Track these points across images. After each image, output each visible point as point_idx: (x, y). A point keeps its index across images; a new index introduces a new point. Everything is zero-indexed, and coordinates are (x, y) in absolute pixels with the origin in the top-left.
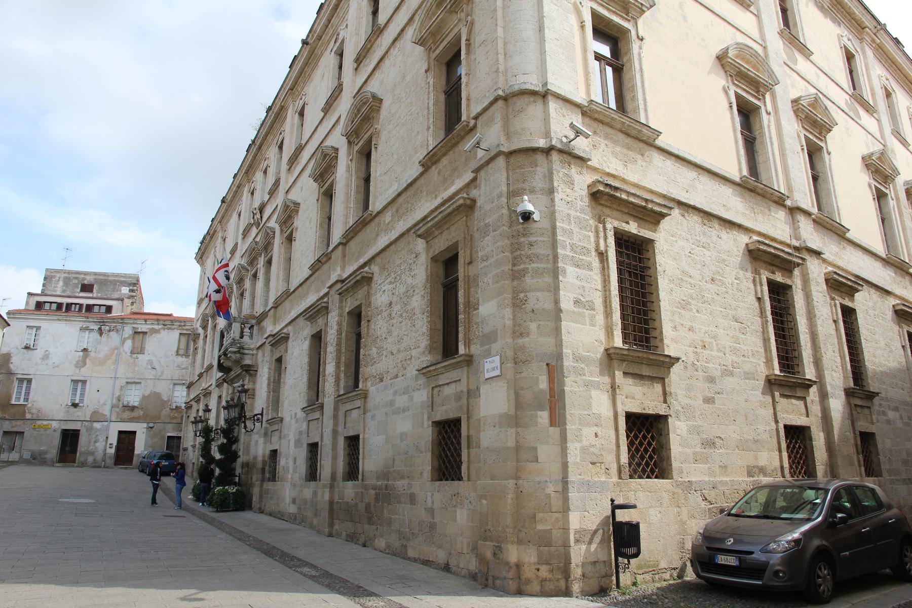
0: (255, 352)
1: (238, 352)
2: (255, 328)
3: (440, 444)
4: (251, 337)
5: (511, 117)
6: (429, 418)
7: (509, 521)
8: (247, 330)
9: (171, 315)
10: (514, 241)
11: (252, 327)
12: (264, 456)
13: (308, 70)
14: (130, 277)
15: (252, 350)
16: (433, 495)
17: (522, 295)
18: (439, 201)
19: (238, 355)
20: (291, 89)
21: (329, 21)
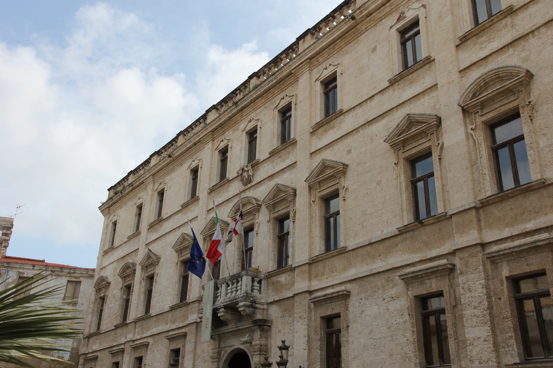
0: (265, 306)
1: (251, 306)
2: (263, 282)
4: (260, 291)
8: (256, 284)
9: (43, 261)
11: (260, 282)
13: (341, 43)
14: (5, 221)
15: (262, 304)
19: (251, 309)
20: (311, 58)
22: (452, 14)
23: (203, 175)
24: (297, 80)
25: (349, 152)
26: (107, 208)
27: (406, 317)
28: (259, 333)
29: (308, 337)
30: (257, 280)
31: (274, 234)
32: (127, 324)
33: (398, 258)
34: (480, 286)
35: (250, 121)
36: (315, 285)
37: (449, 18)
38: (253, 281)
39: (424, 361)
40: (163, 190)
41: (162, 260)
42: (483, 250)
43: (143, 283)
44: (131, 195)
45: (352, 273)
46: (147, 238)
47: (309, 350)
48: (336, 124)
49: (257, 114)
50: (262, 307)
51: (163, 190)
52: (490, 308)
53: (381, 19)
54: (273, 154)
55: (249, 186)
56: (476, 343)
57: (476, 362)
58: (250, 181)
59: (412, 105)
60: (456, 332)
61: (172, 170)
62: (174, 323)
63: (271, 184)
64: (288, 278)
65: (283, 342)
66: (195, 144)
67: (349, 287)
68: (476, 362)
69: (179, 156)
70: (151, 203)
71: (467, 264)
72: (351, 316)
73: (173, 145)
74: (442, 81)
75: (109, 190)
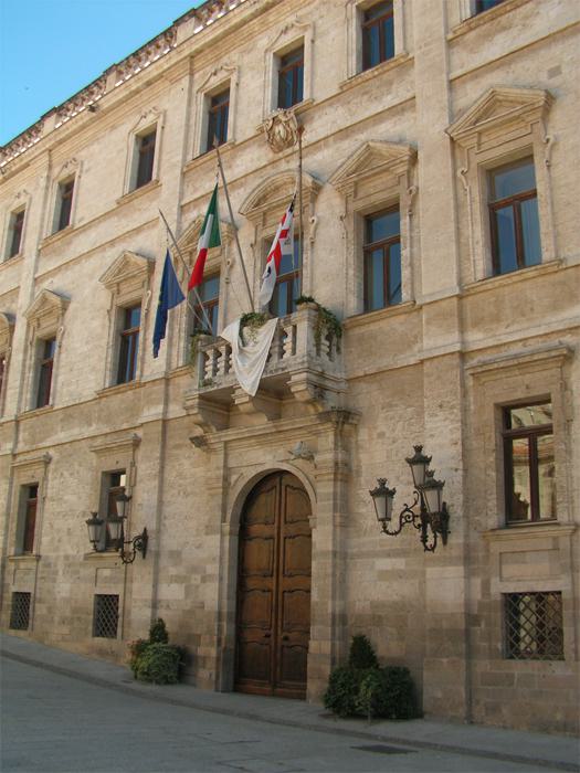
0: (343, 386)
12: (467, 604)
15: (336, 381)
28: (331, 438)
35: (285, 31)
41: (72, 306)
43: (32, 352)
50: (335, 386)
54: (346, 89)
61: (95, 139)
63: (350, 146)
65: (419, 449)
66: (149, 84)
69: (111, 109)
73: (92, 93)
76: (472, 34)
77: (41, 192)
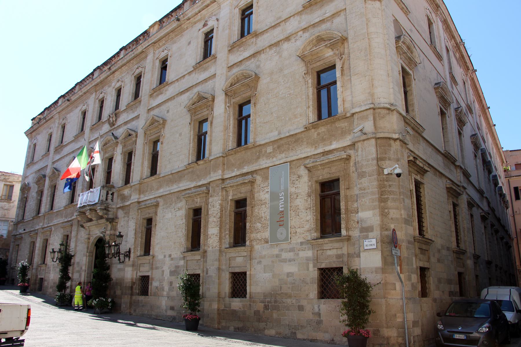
1: (105, 209)
3: (322, 280)
4: (112, 200)
5: (378, 119)
6: (314, 267)
7: (384, 318)
10: (381, 183)
12: (132, 279)
13: (172, 35)
16: (319, 306)
17: (386, 211)
18: (320, 150)
20: (154, 43)
21: (200, 12)
22: (230, 29)
23: (89, 116)
24: (146, 57)
25: (168, 111)
26: (30, 133)
27: (184, 220)
29: (136, 230)
30: (110, 192)
31: (124, 163)
32: (40, 217)
33: (185, 185)
34: (218, 204)
35: (118, 82)
36: (143, 198)
37: (227, 32)
38: (107, 194)
39: (190, 246)
40: (65, 124)
42: (223, 183)
43: (50, 190)
44: (45, 125)
45: (162, 191)
46: (53, 158)
47: (136, 238)
48: (164, 92)
49: (123, 77)
51: (65, 124)
52: (221, 217)
53: (195, 23)
55: (113, 127)
56: (212, 237)
57: (211, 247)
58: (114, 125)
59: (203, 85)
60: (205, 230)
61: (71, 111)
62: (66, 218)
64: (129, 192)
65: (120, 233)
66: (85, 93)
67: (159, 199)
68: (211, 247)
69: (75, 101)
70: (57, 133)
71: (214, 191)
72: (158, 219)
74: (218, 73)
75: (32, 120)
76: (155, 94)
77: (56, 128)
